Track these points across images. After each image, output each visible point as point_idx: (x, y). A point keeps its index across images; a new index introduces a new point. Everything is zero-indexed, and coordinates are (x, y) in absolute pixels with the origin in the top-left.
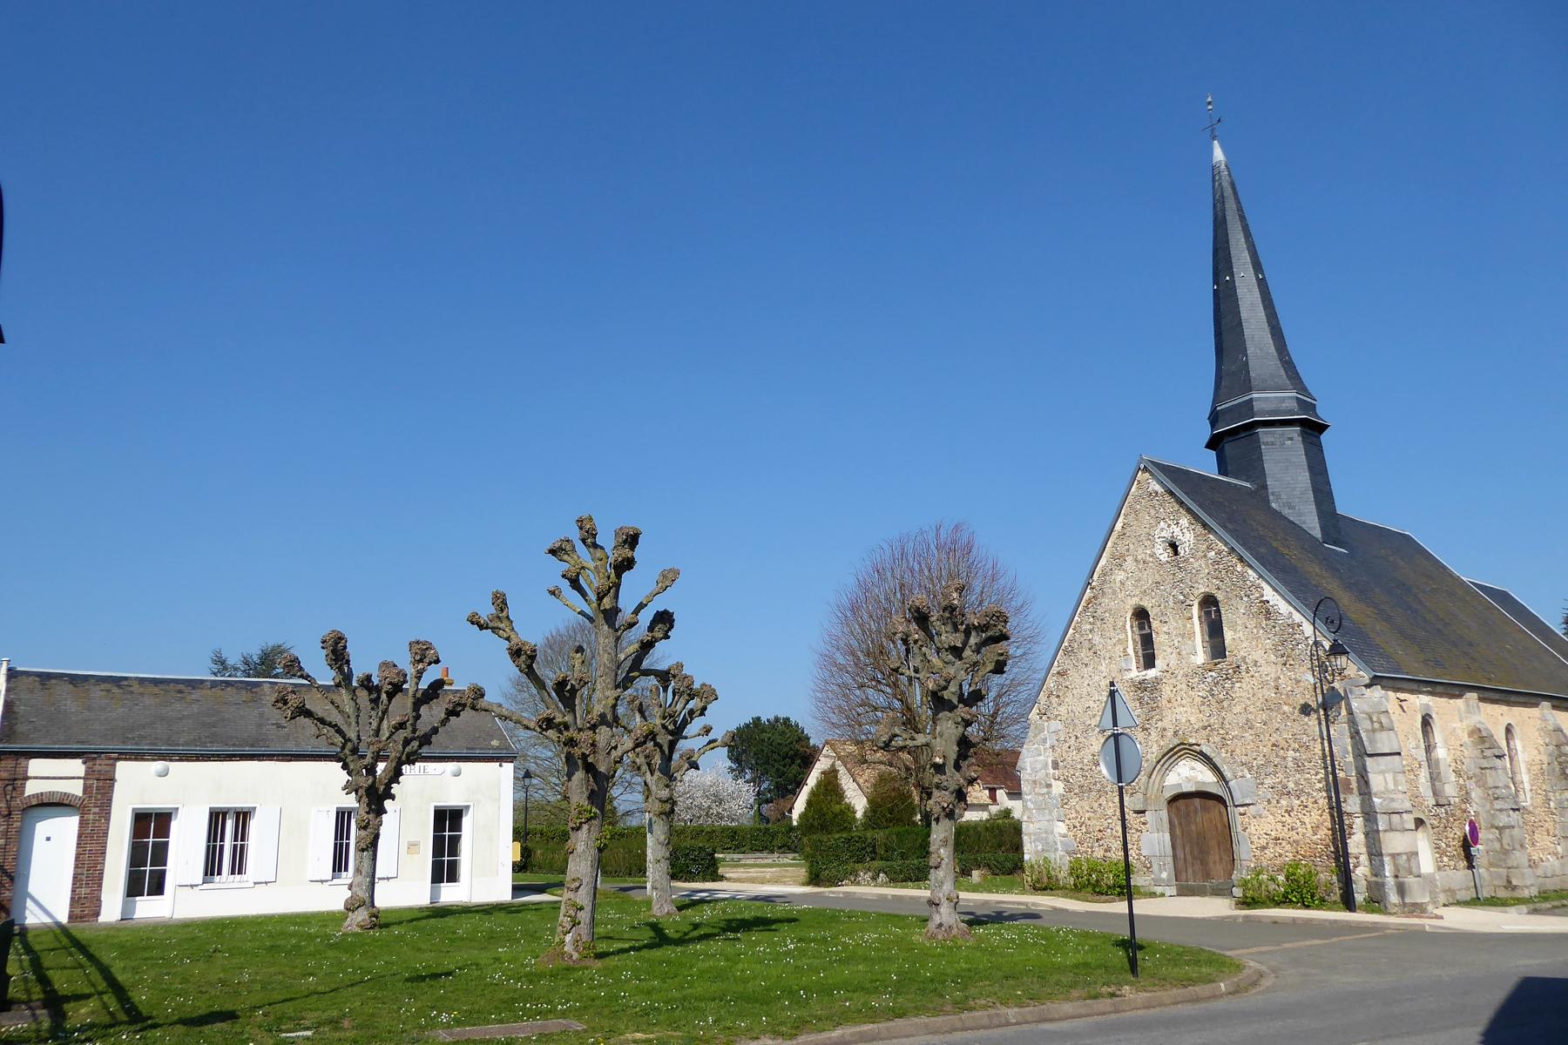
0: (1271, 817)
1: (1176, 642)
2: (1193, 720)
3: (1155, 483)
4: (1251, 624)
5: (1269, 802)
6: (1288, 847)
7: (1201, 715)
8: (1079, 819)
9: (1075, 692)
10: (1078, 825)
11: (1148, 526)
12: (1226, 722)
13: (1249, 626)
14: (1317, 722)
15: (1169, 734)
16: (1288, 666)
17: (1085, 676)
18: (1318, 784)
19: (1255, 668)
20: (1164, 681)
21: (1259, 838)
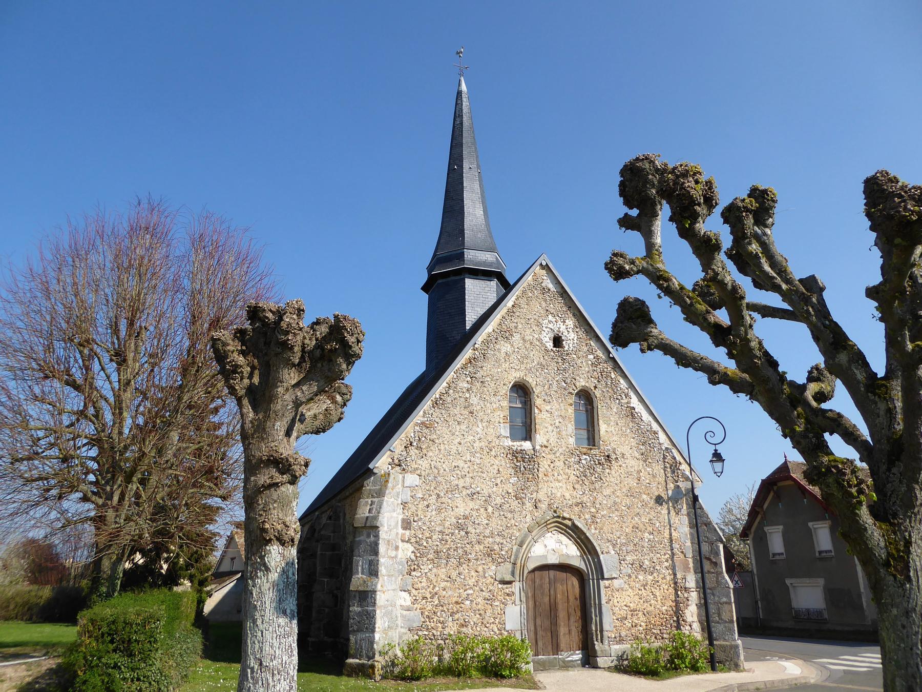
0: (630, 590)
1: (557, 421)
2: (567, 496)
3: (549, 281)
4: (621, 423)
5: (630, 576)
6: (643, 618)
7: (575, 493)
8: (430, 589)
9: (442, 447)
10: (428, 596)
11: (538, 314)
12: (597, 502)
13: (620, 424)
14: (667, 512)
15: (543, 506)
16: (647, 463)
17: (457, 433)
18: (665, 563)
19: (622, 460)
20: (543, 454)
21: (620, 610)
